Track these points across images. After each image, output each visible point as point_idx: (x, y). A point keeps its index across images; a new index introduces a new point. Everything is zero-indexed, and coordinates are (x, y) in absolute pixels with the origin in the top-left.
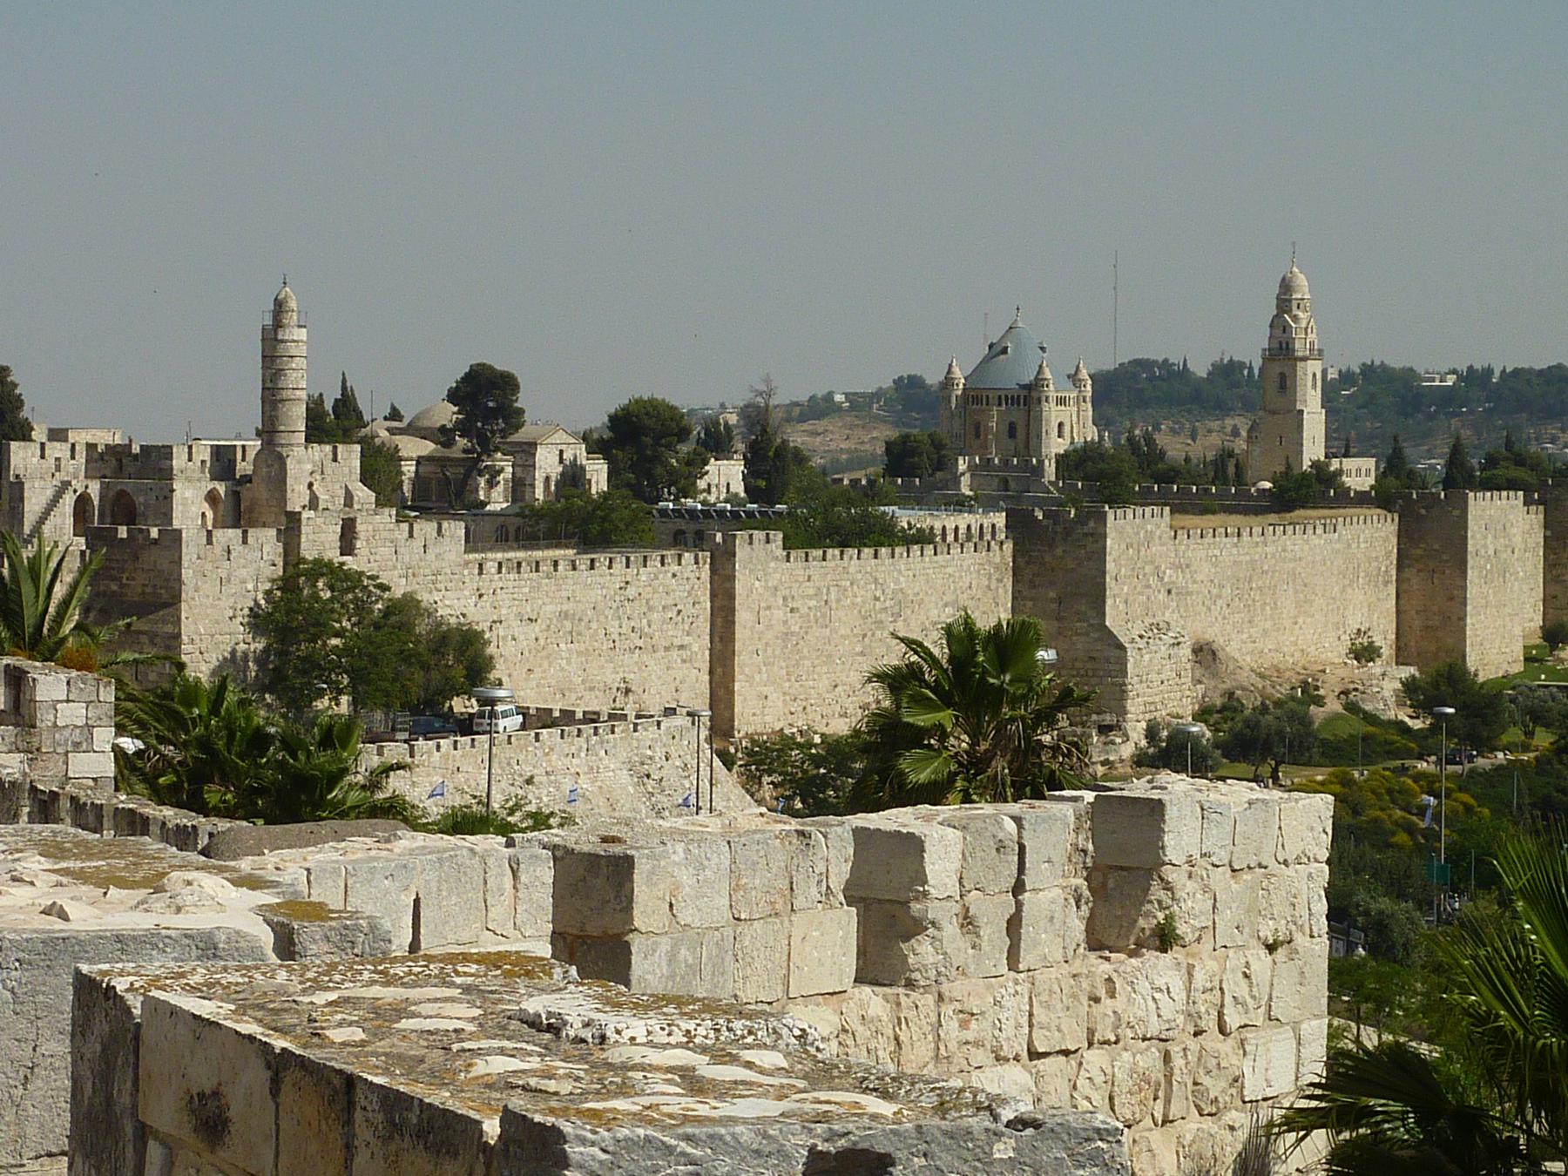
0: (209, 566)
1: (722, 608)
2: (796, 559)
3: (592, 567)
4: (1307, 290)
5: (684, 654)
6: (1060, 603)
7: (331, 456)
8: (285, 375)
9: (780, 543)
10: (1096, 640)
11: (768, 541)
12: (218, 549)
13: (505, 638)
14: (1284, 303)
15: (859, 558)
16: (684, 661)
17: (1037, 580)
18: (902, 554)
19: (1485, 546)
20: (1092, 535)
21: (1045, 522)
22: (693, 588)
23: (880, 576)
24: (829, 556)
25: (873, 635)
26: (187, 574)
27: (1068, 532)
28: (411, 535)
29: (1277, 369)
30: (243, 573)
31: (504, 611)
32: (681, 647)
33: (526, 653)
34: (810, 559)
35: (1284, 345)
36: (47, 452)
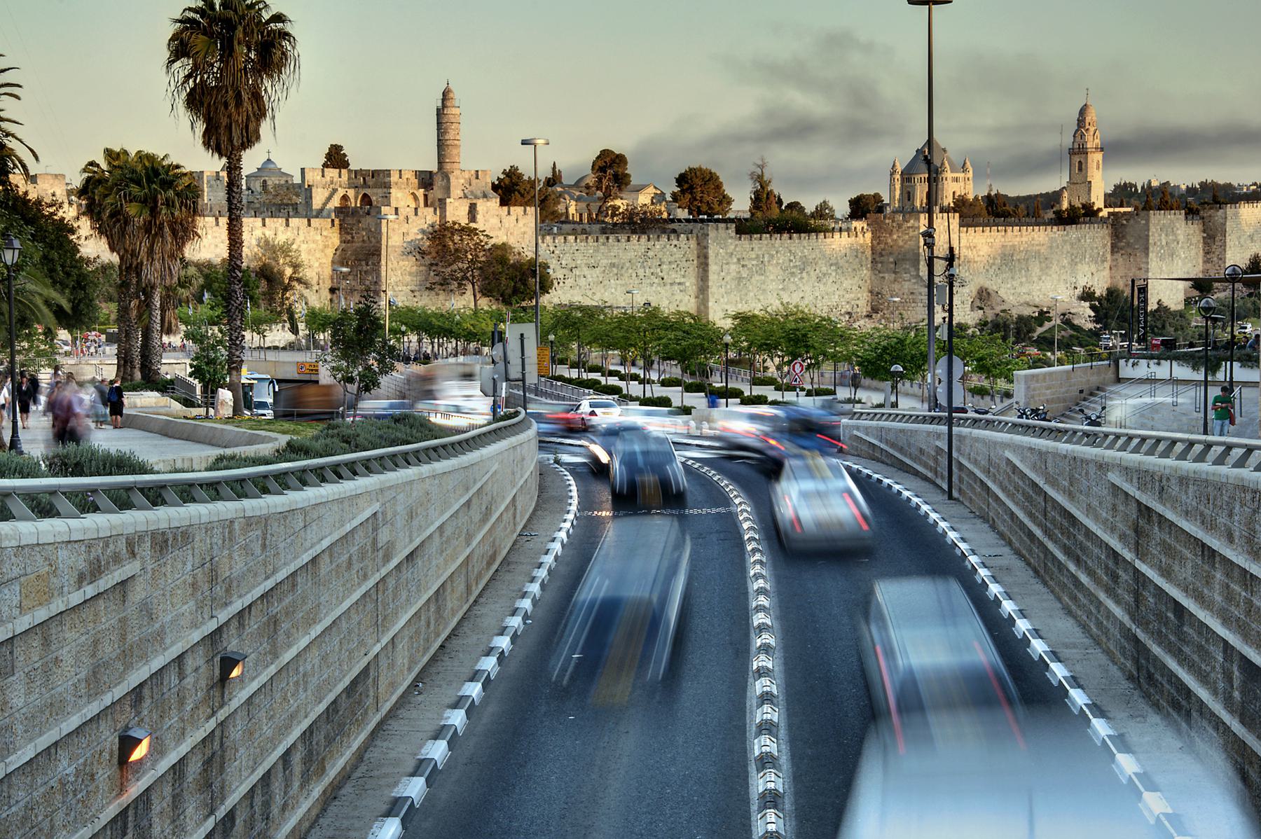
2: (745, 239)
3: (629, 241)
5: (682, 287)
7: (475, 176)
9: (734, 229)
10: (915, 283)
11: (727, 228)
13: (579, 276)
16: (681, 291)
19: (1160, 240)
20: (912, 227)
23: (793, 249)
24: (763, 238)
27: (900, 226)
28: (509, 213)
29: (1076, 159)
31: (579, 262)
32: (679, 284)
33: (592, 284)
36: (326, 174)
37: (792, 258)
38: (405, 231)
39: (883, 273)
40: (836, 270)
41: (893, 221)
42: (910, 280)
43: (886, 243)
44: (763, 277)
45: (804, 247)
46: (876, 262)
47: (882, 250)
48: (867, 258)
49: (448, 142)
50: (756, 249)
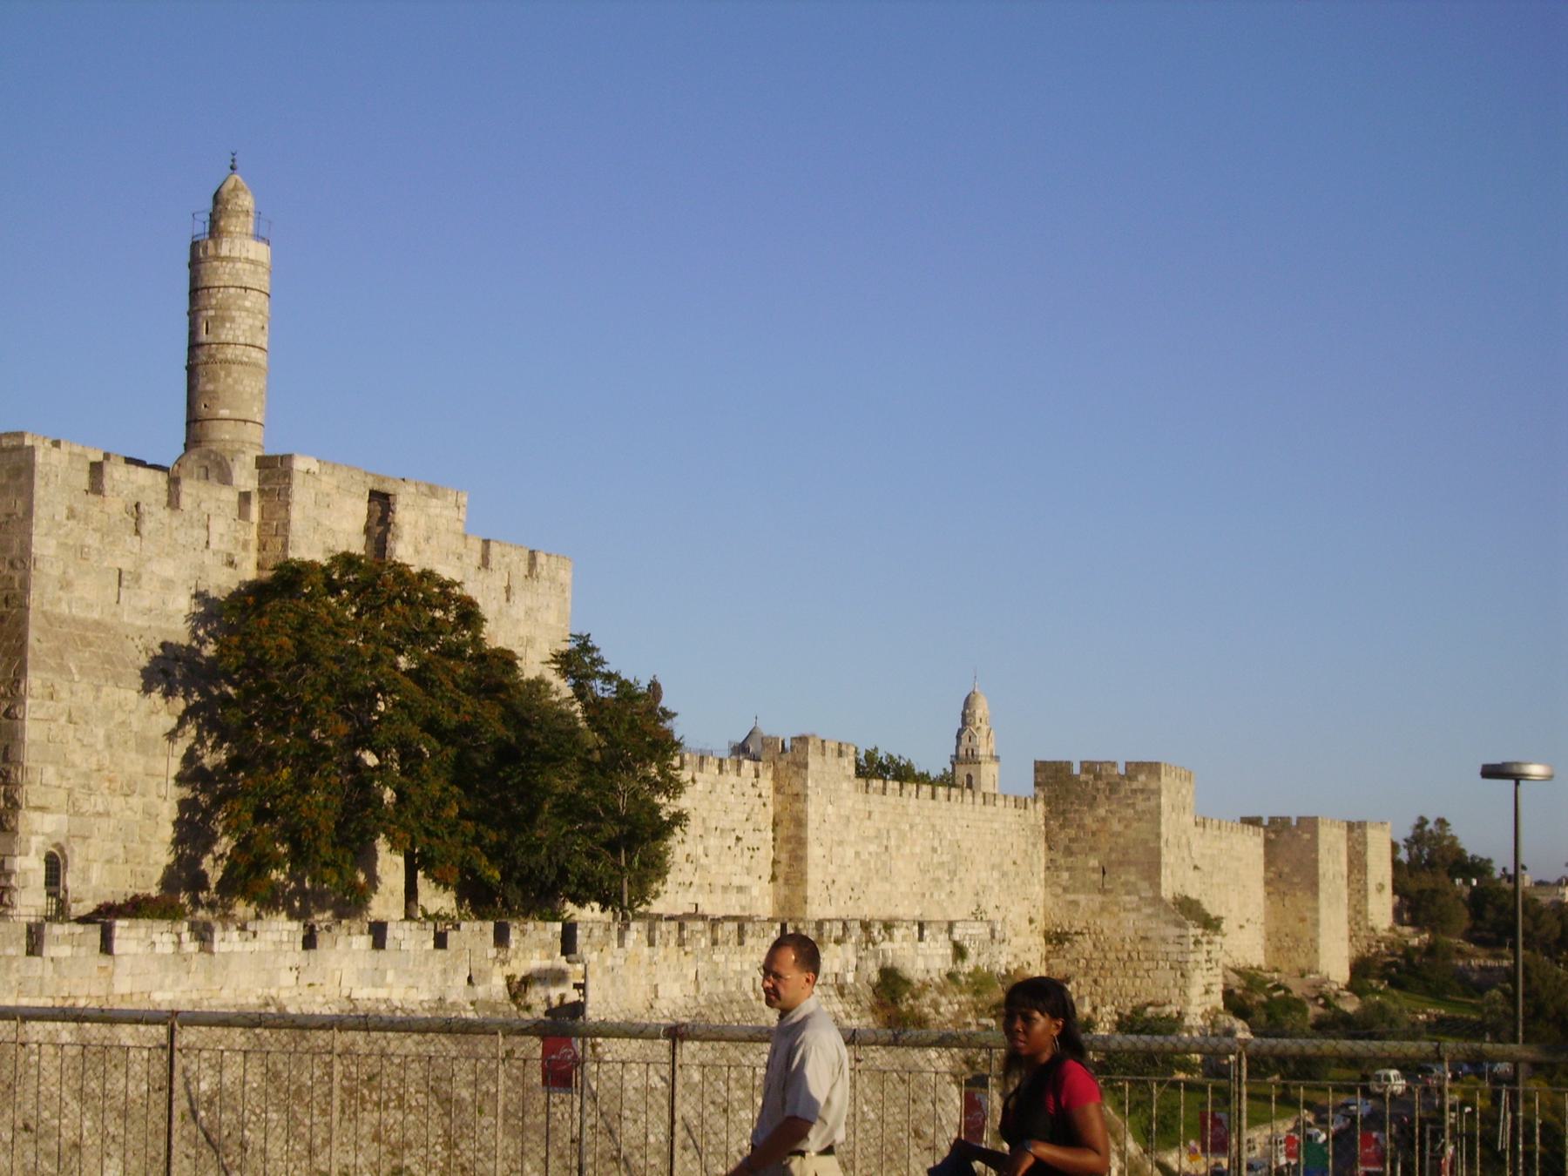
0: (92, 540)
1: (787, 840)
4: (986, 706)
6: (1104, 873)
8: (233, 320)
10: (1150, 916)
12: (115, 505)
14: (966, 719)
15: (917, 797)
17: (1075, 846)
18: (957, 798)
20: (1142, 791)
21: (1083, 777)
22: (752, 809)
23: (938, 822)
24: (889, 791)
25: (932, 895)
26: (44, 544)
27: (1113, 788)
30: (167, 569)
32: (740, 889)
34: (871, 790)
35: (970, 752)
37: (936, 843)
38: (126, 565)
39: (1075, 891)
40: (999, 881)
41: (1098, 777)
42: (1138, 909)
43: (1081, 827)
44: (887, 886)
45: (956, 819)
46: (1057, 869)
47: (1071, 840)
48: (1039, 858)
49: (230, 352)
50: (876, 816)
